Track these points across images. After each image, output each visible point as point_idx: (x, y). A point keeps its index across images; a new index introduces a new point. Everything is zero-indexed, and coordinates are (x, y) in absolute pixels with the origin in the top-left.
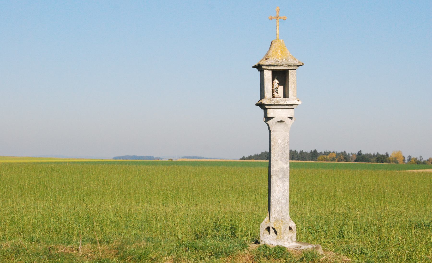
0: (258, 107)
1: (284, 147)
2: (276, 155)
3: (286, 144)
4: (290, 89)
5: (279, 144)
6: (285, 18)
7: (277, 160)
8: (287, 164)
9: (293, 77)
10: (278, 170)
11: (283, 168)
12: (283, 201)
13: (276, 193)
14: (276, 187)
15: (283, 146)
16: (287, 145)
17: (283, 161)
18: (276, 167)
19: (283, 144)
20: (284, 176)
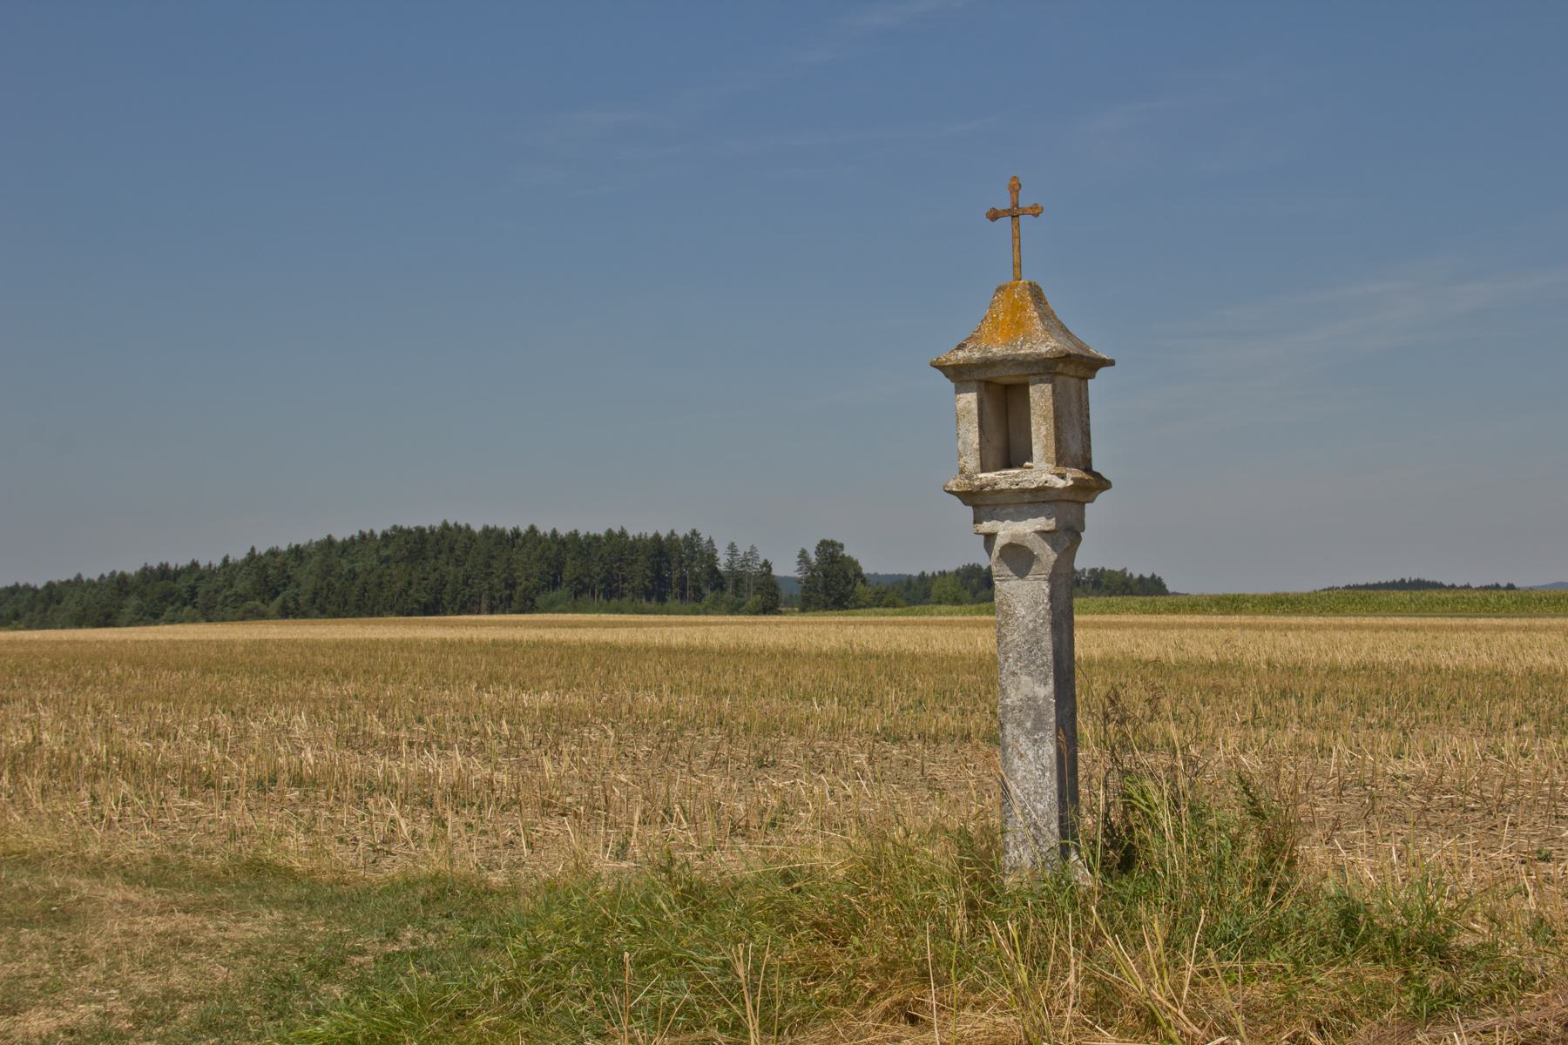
1: (1035, 629)
4: (1034, 441)
6: (1037, 211)
7: (1014, 674)
8: (1045, 684)
11: (1035, 699)
12: (1039, 806)
13: (1016, 779)
14: (1016, 760)
17: (1032, 676)
19: (1031, 618)
20: (1039, 725)
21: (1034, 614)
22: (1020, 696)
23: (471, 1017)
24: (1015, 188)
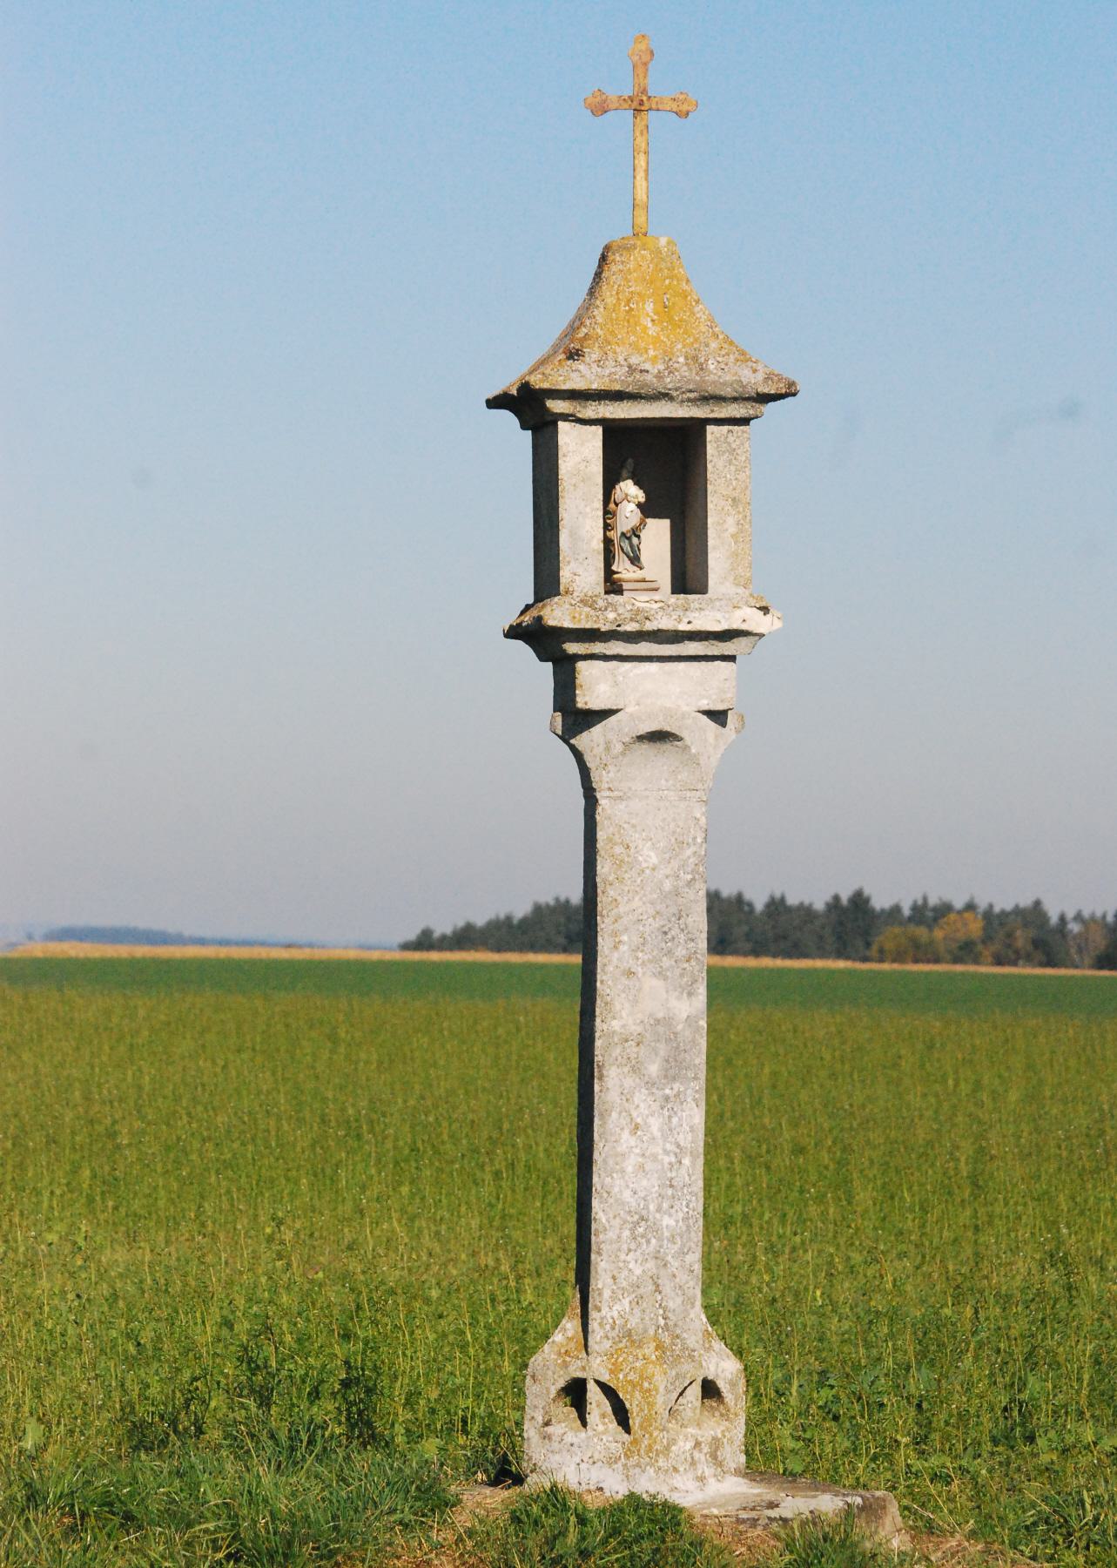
0: (522, 649)
2: (625, 938)
3: (689, 877)
4: (711, 542)
5: (647, 871)
6: (685, 108)
7: (630, 973)
8: (690, 994)
9: (733, 468)
10: (639, 1029)
12: (667, 1221)
13: (623, 1171)
14: (626, 1135)
15: (668, 885)
16: (694, 879)
17: (666, 979)
18: (624, 1014)
19: (668, 871)
20: (674, 1069)
21: (675, 864)
22: (640, 1016)
23: (375, 1385)
24: (642, 65)
